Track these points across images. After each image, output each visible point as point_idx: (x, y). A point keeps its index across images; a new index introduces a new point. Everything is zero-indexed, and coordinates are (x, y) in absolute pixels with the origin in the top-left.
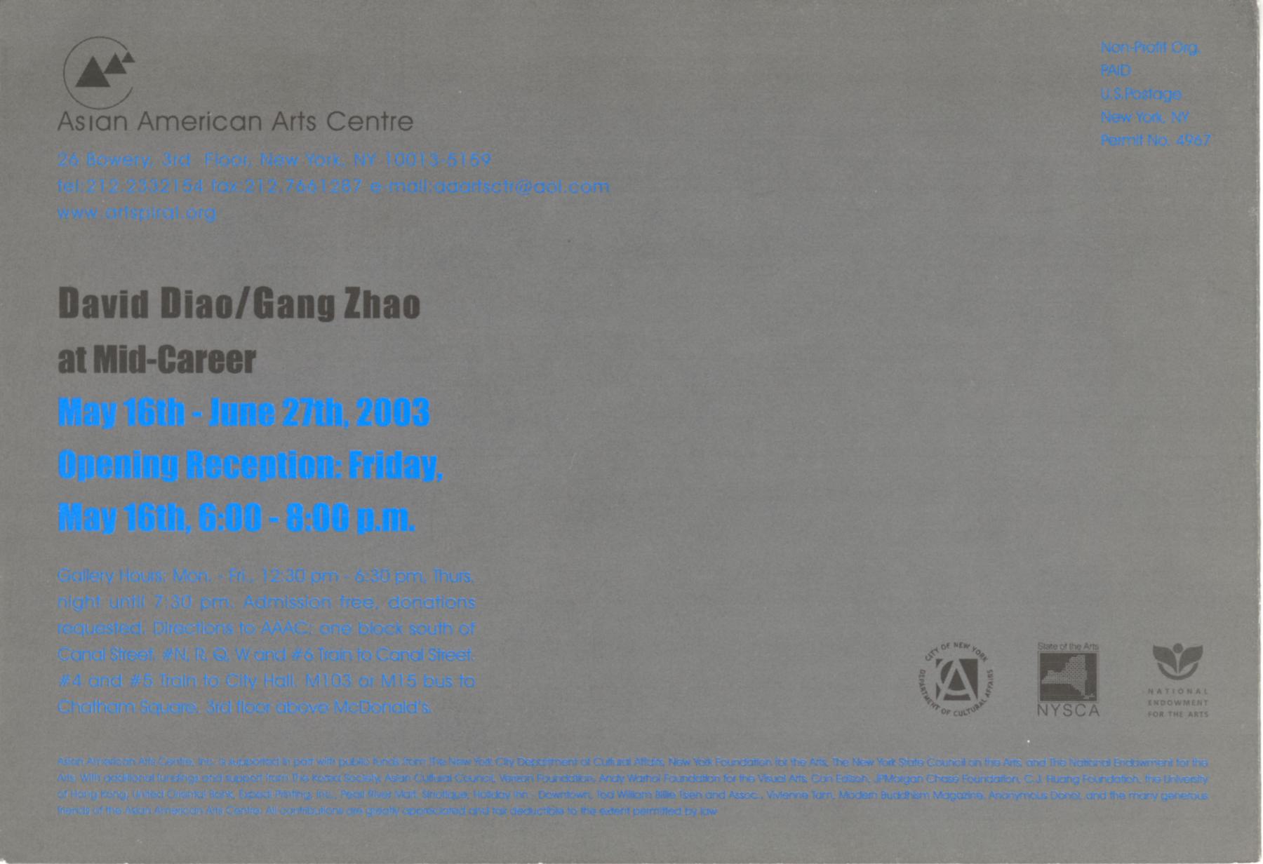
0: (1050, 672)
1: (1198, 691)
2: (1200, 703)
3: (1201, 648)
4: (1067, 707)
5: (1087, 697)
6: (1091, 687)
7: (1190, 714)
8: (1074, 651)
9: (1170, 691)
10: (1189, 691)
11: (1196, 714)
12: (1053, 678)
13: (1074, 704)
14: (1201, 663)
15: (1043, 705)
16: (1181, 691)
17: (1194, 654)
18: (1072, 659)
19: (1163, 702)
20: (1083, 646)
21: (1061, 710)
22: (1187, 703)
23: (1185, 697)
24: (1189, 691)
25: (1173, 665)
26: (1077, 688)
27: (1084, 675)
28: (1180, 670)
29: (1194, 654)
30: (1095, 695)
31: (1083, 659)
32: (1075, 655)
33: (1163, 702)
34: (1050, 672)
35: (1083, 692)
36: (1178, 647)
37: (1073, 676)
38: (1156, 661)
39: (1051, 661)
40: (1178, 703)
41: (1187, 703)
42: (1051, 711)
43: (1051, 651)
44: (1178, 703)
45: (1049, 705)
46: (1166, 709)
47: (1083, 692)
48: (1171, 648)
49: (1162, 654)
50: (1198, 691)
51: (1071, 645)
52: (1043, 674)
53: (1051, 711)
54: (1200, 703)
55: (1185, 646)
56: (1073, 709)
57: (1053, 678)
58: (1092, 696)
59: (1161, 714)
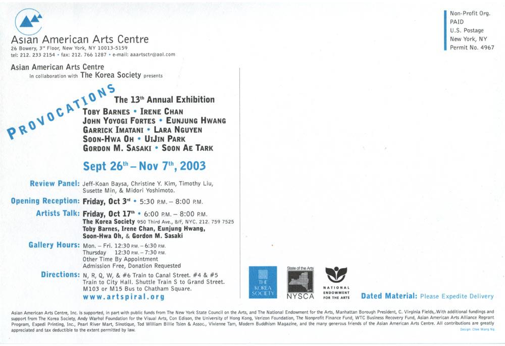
0: (292, 279)
1: (345, 288)
2: (346, 293)
3: (346, 268)
4: (300, 295)
5: (308, 291)
6: (310, 287)
7: (342, 298)
8: (303, 270)
9: (333, 288)
10: (341, 288)
11: (344, 298)
12: (293, 282)
13: (303, 294)
14: (346, 275)
15: (289, 294)
16: (338, 288)
17: (343, 272)
18: (303, 274)
19: (330, 293)
20: (307, 268)
21: (297, 296)
22: (340, 293)
23: (340, 290)
24: (341, 288)
25: (335, 277)
26: (304, 286)
27: (307, 280)
28: (338, 278)
29: (343, 272)
30: (312, 289)
31: (306, 274)
32: (303, 272)
33: (330, 293)
34: (292, 279)
35: (307, 289)
36: (336, 268)
37: (303, 281)
38: (327, 275)
39: (293, 275)
40: (336, 293)
41: (340, 293)
42: (293, 296)
43: (293, 270)
44: (336, 293)
45: (292, 294)
46: (331, 295)
47: (307, 289)
48: (334, 269)
49: (329, 272)
50: (345, 288)
51: (302, 268)
52: (289, 280)
53: (293, 296)
54: (346, 293)
55: (339, 269)
56: (302, 296)
57: (293, 282)
58: (311, 290)
59: (329, 298)
